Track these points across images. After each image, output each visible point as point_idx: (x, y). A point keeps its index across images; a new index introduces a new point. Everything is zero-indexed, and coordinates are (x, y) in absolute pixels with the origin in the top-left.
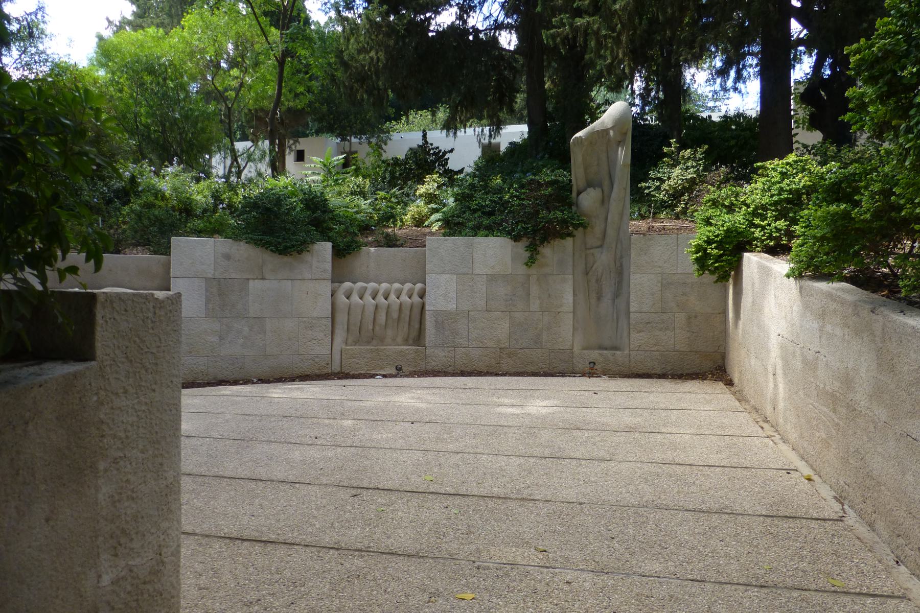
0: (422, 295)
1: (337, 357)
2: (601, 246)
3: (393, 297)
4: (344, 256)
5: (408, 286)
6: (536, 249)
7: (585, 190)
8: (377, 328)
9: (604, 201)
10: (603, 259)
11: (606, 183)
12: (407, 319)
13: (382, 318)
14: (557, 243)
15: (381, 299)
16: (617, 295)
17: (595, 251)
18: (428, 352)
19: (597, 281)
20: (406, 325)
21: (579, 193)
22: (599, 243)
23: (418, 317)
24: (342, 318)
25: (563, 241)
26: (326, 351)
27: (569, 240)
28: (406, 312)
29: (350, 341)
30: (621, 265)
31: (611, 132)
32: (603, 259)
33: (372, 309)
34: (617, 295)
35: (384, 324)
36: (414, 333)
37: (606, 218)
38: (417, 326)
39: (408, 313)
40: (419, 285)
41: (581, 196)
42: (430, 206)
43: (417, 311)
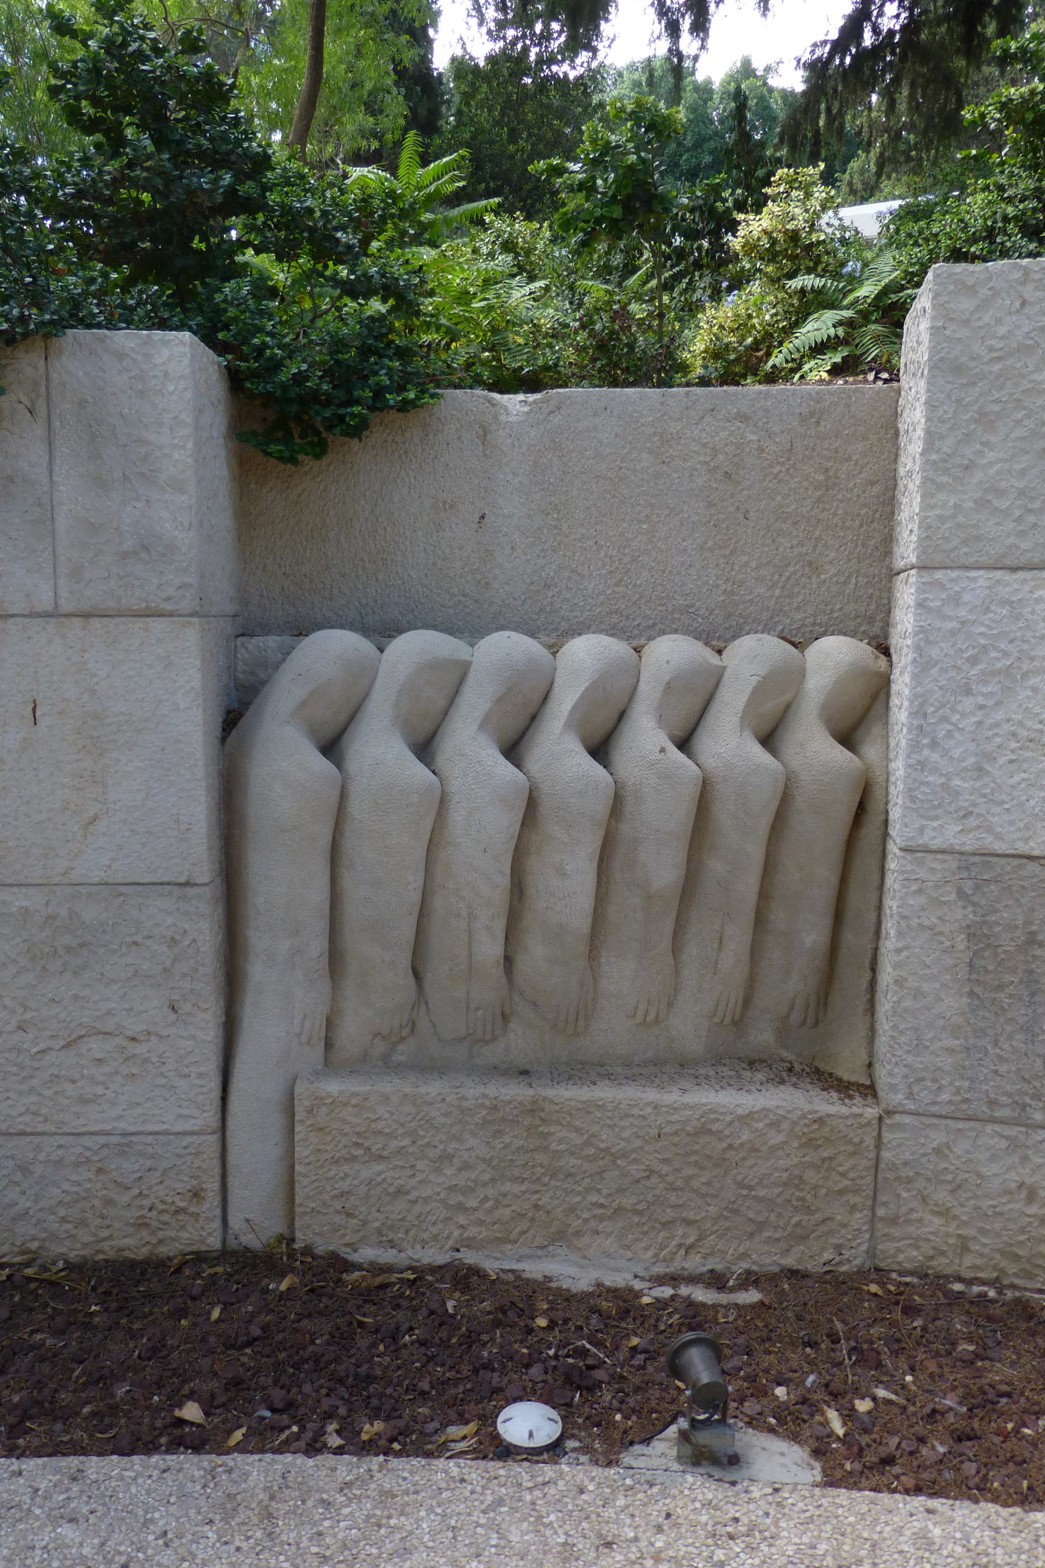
0: (856, 721)
1: (255, 1153)
3: (646, 739)
4: (320, 450)
5: (752, 655)
8: (535, 954)
12: (748, 886)
13: (567, 881)
15: (560, 753)
18: (901, 1145)
20: (738, 936)
23: (826, 874)
24: (284, 885)
26: (182, 1106)
28: (740, 845)
29: (353, 1032)
33: (501, 824)
35: (580, 920)
36: (789, 983)
38: (813, 936)
39: (755, 851)
40: (834, 655)
42: (796, 283)
43: (819, 834)
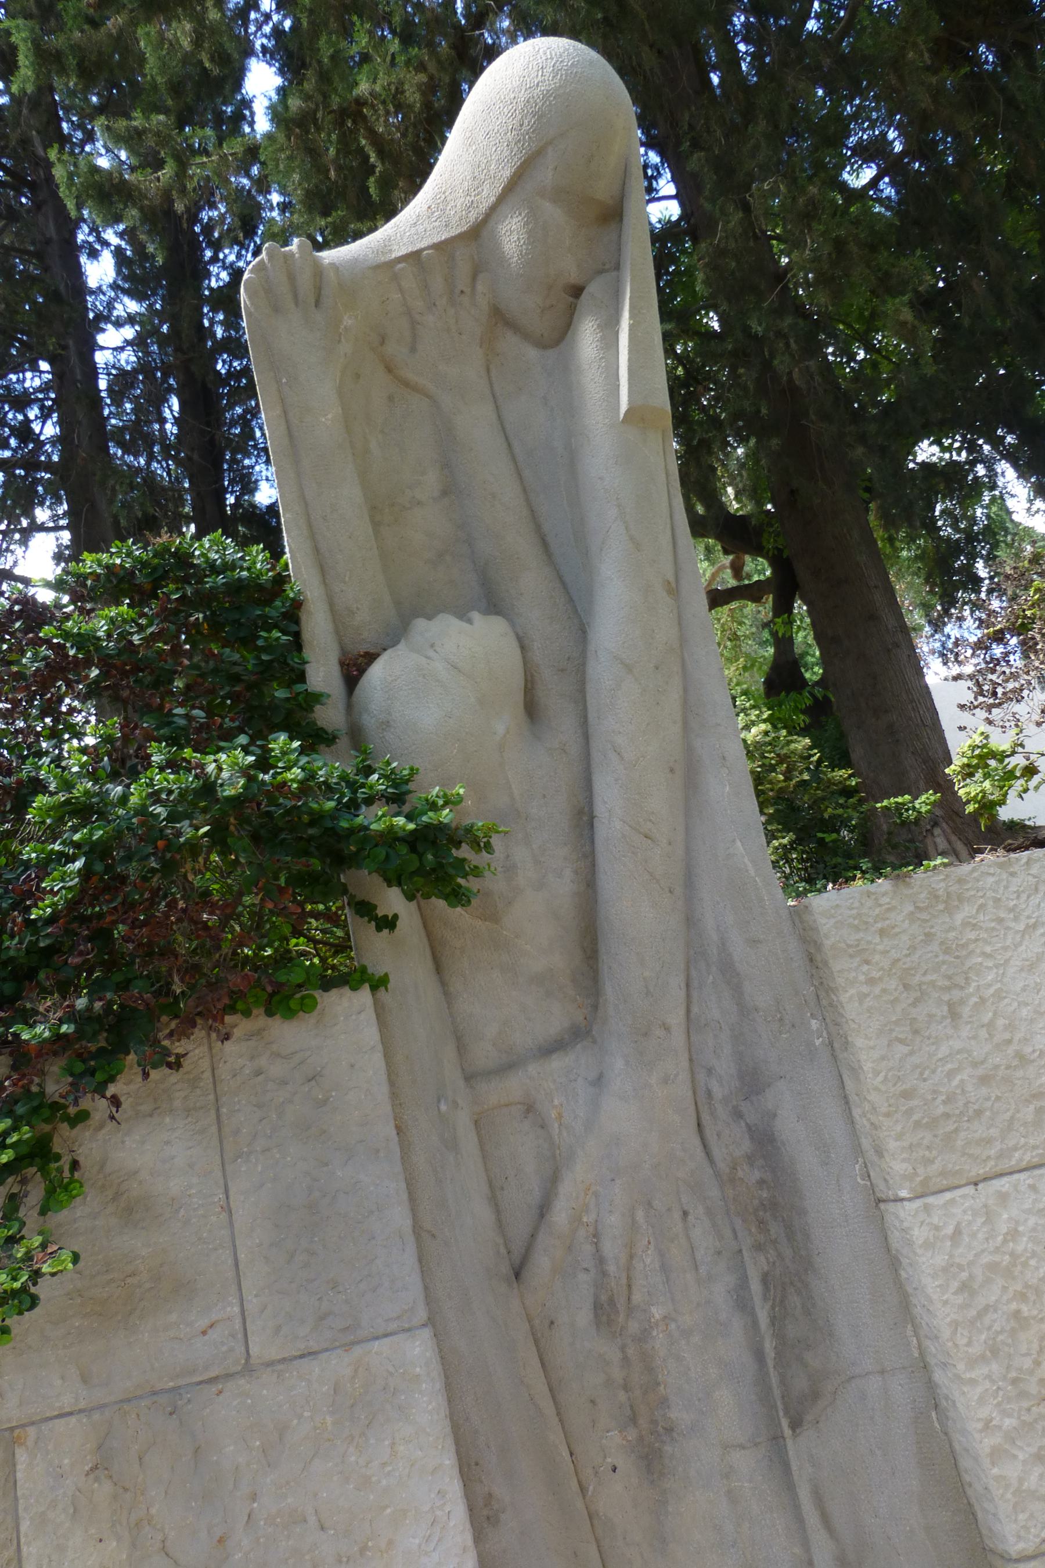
2: (580, 1034)
6: (39, 1153)
7: (395, 634)
9: (547, 695)
10: (622, 1125)
11: (531, 585)
14: (244, 1058)
16: (792, 1392)
17: (554, 1080)
19: (605, 1313)
21: (354, 669)
22: (556, 1017)
25: (288, 1034)
27: (349, 1010)
30: (765, 1144)
31: (512, 235)
32: (622, 1125)
34: (792, 1392)
37: (584, 819)
41: (376, 672)
